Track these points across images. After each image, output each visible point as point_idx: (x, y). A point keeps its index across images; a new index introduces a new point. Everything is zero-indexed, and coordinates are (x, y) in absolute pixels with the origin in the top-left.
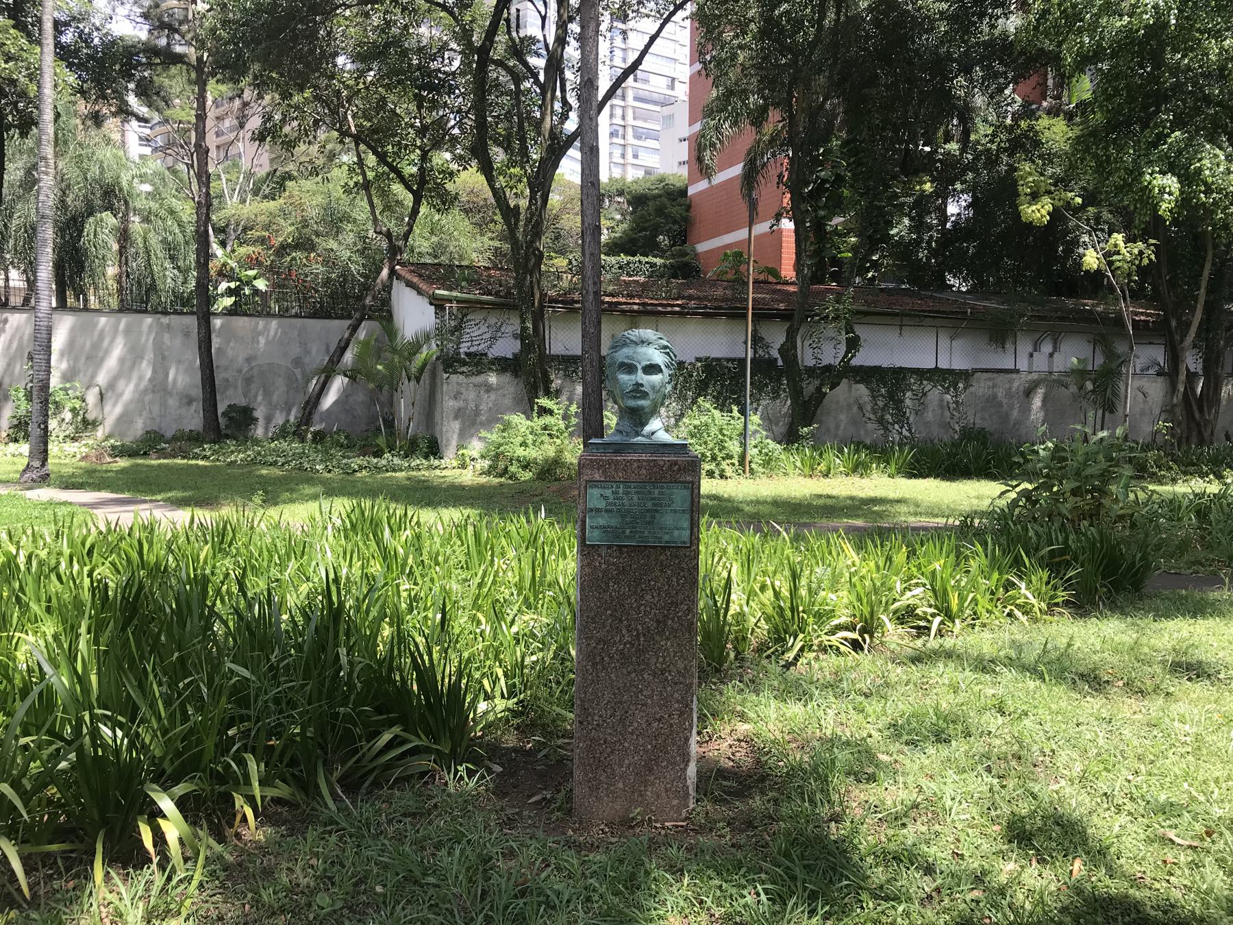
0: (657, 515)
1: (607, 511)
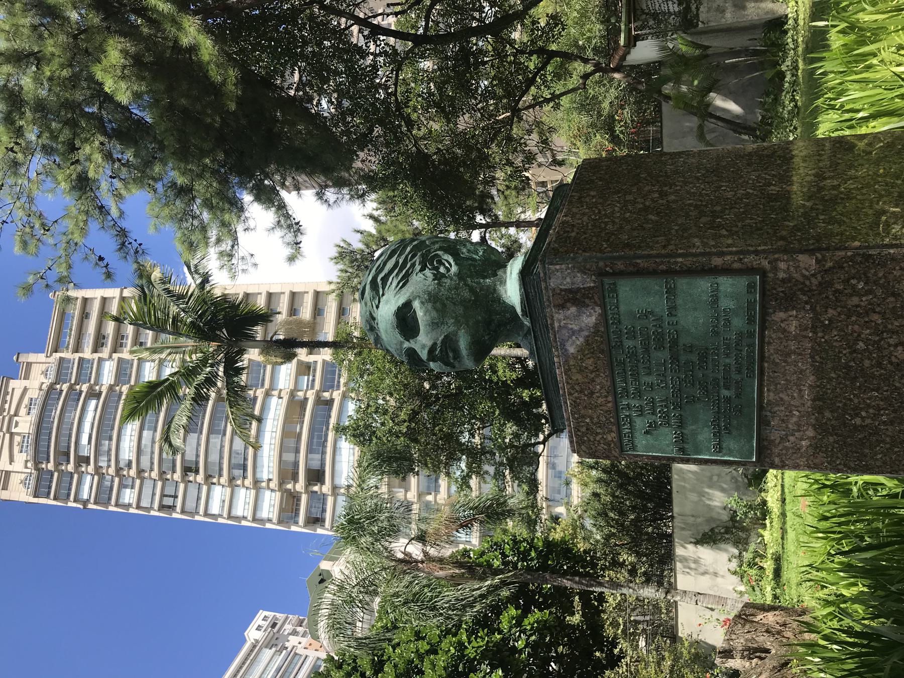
0: (684, 340)
1: (681, 424)
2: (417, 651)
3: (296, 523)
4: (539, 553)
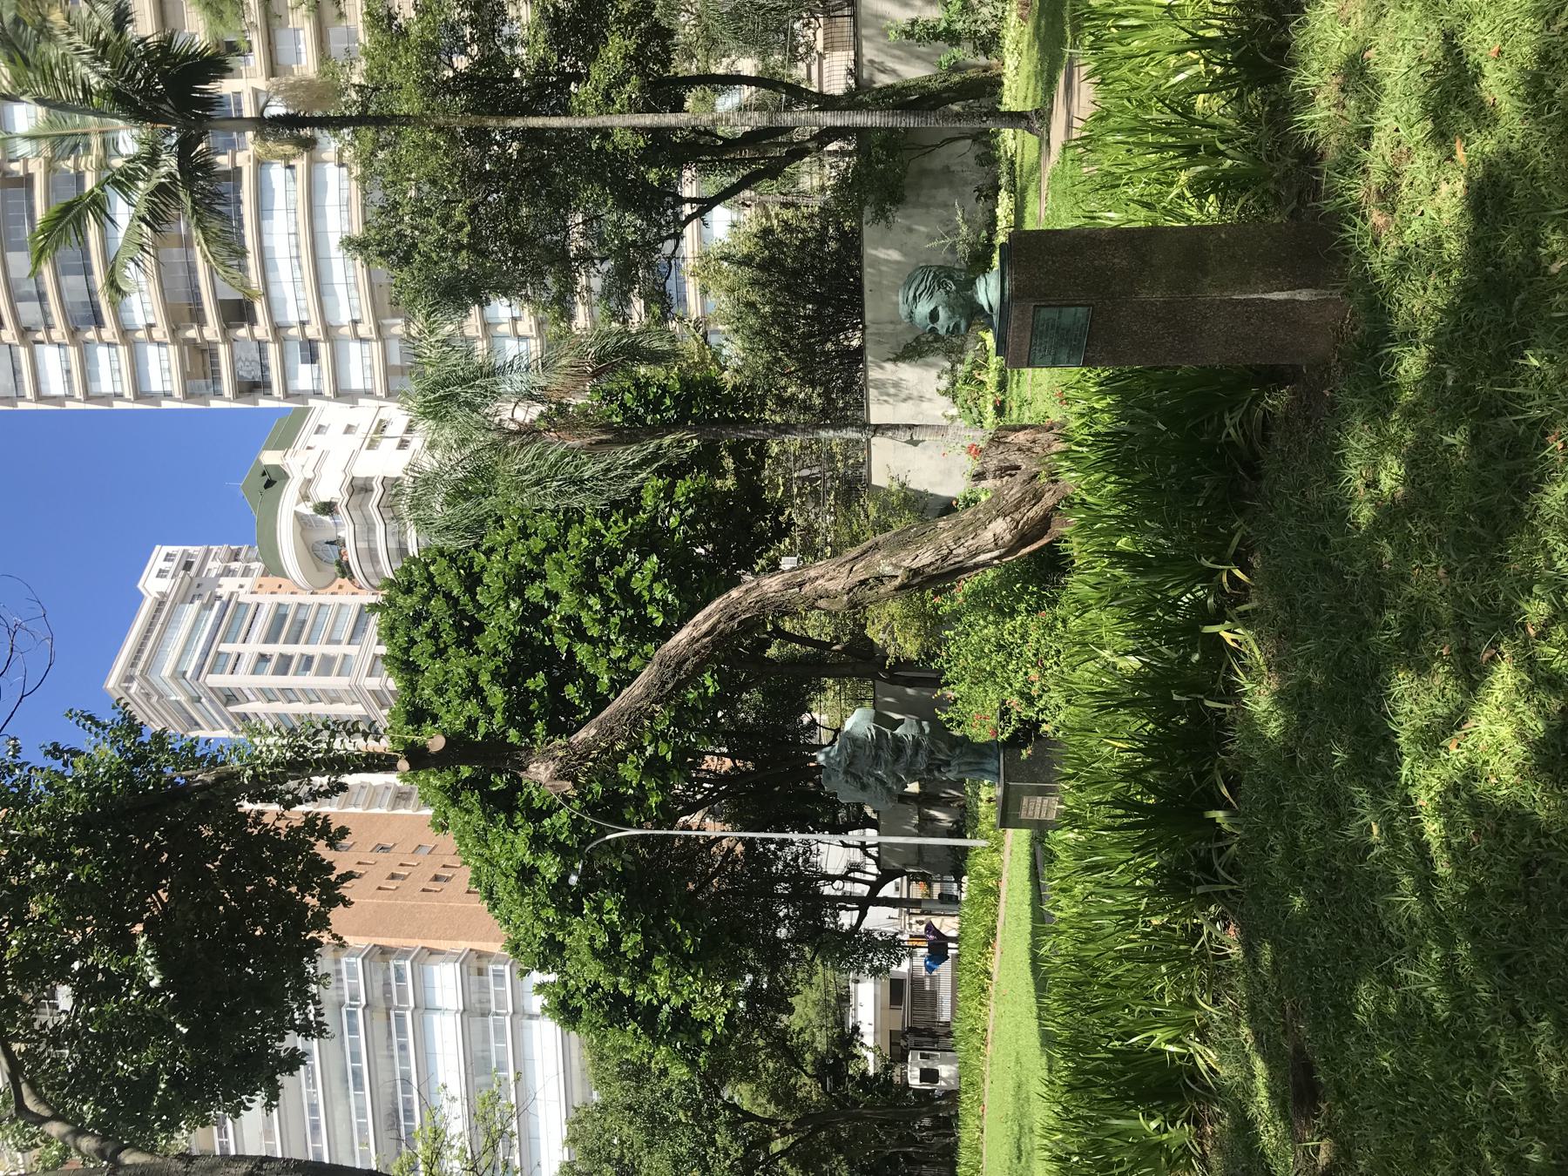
2: (530, 553)
3: (218, 394)
4: (676, 399)
